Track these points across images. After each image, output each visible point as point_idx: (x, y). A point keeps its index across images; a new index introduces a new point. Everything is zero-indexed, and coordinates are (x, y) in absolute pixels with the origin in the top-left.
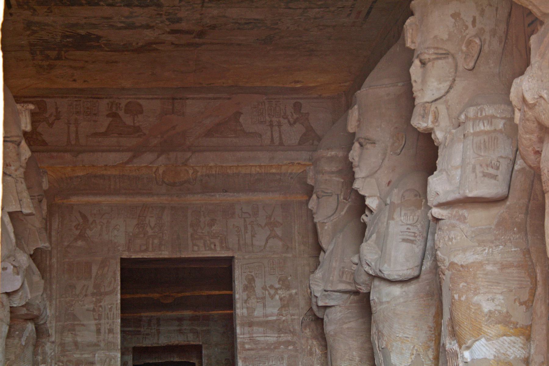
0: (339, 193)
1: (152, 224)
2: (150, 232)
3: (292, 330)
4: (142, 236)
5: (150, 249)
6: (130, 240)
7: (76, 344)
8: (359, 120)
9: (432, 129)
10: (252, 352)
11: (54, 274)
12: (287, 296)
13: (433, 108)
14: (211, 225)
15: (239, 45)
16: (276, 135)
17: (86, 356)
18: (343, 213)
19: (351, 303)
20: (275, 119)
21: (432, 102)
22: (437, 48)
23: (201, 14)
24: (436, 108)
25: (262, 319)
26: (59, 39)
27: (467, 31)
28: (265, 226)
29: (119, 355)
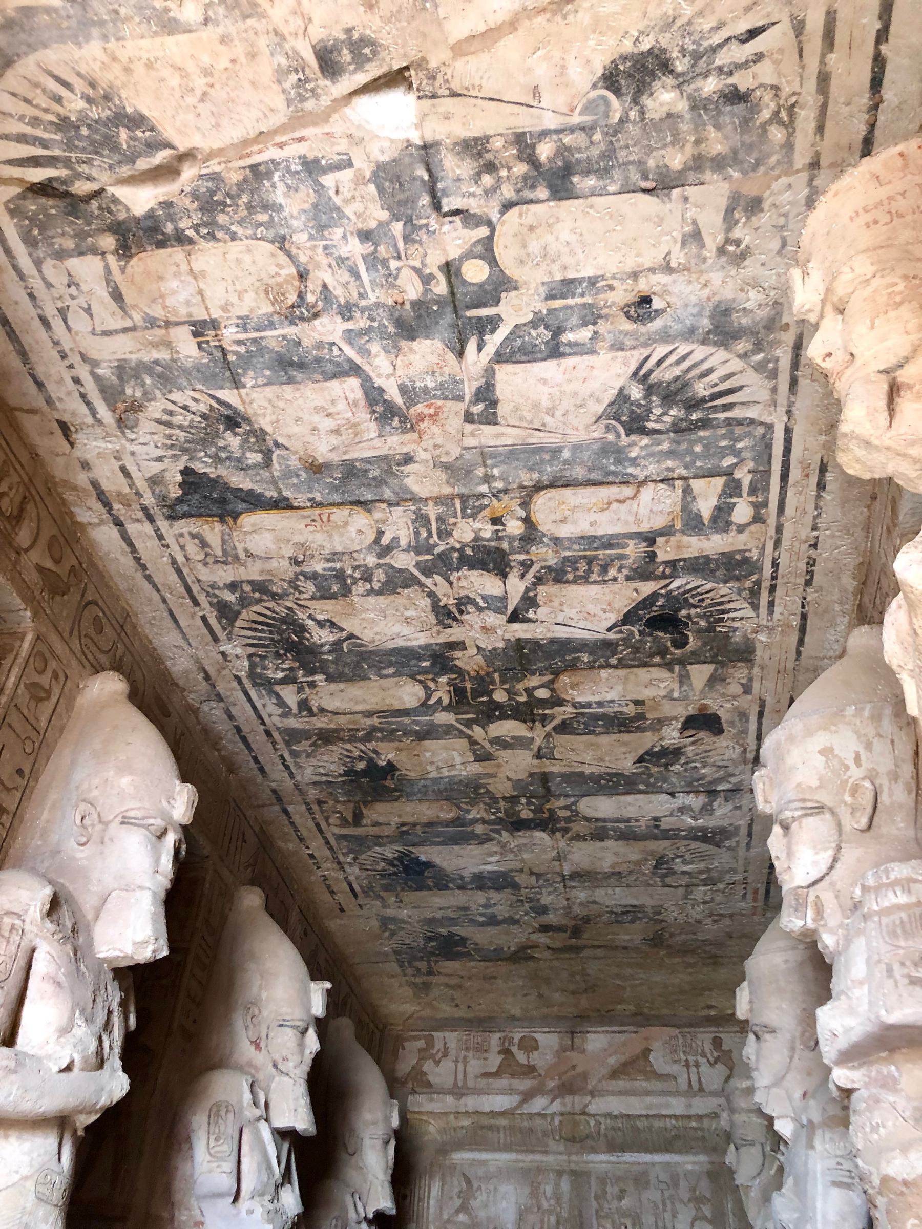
0: (763, 1141)
2: (545, 1205)
6: (521, 1215)
8: (751, 1002)
9: (815, 932)
13: (811, 898)
14: (620, 1199)
15: (625, 948)
16: (694, 1078)
20: (691, 1058)
21: (808, 887)
22: (804, 800)
23: (568, 899)
24: (817, 897)
26: (422, 942)
27: (849, 773)
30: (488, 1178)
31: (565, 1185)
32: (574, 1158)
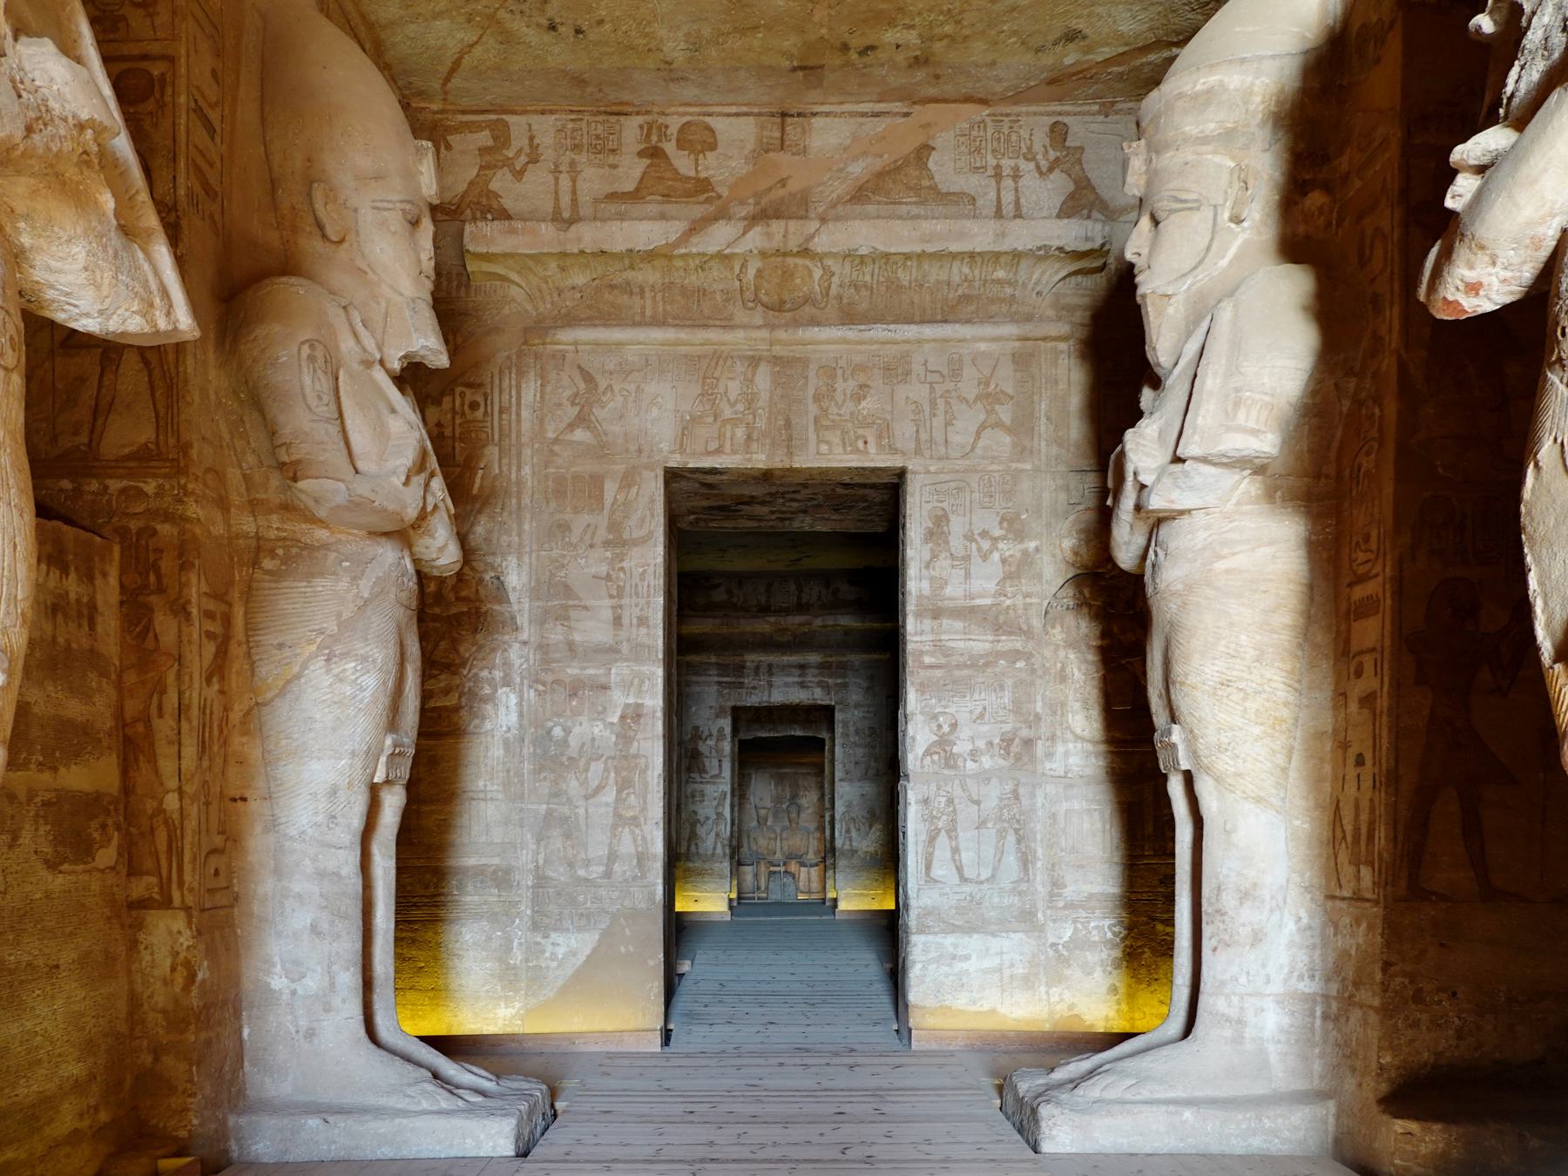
1: (733, 396)
2: (728, 413)
3: (1025, 627)
4: (711, 419)
5: (728, 448)
6: (684, 428)
7: (571, 646)
10: (938, 673)
11: (526, 500)
12: (1018, 555)
14: (858, 398)
17: (592, 671)
18: (1224, 263)
19: (1238, 503)
25: (962, 603)
28: (975, 401)
29: (659, 672)
30: (625, 371)
31: (763, 380)
32: (782, 335)
